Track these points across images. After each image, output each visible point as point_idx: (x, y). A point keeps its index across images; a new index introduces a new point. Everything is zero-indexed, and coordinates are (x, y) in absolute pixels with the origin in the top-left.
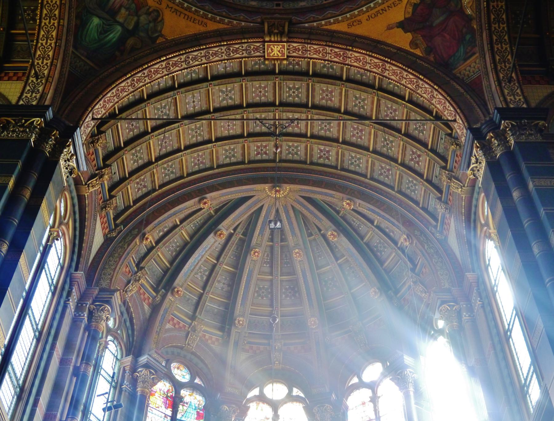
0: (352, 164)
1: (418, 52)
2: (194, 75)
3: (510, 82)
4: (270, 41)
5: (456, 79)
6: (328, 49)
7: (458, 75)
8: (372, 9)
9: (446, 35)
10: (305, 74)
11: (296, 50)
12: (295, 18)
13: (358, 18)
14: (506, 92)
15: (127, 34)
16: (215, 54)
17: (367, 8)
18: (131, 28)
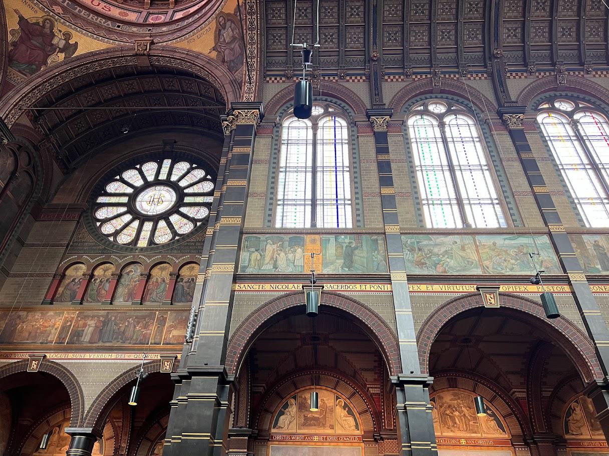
1: (10, 38)
3: (19, 109)
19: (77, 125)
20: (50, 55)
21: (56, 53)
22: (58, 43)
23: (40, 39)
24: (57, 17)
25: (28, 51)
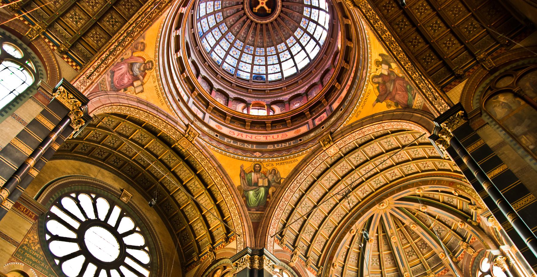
0: (408, 170)
1: (393, 108)
2: (308, 183)
3: (436, 100)
4: (327, 149)
5: (416, 111)
6: (354, 134)
7: (415, 108)
8: (361, 102)
9: (399, 92)
10: (356, 148)
11: (340, 144)
12: (332, 130)
13: (358, 110)
14: (436, 106)
15: (267, 188)
16: (308, 170)
17: (359, 103)
18: (267, 185)
19: (450, 40)
20: (396, 75)
21: (393, 70)
22: (385, 70)
23: (388, 84)
24: (368, 74)
25: (399, 93)
